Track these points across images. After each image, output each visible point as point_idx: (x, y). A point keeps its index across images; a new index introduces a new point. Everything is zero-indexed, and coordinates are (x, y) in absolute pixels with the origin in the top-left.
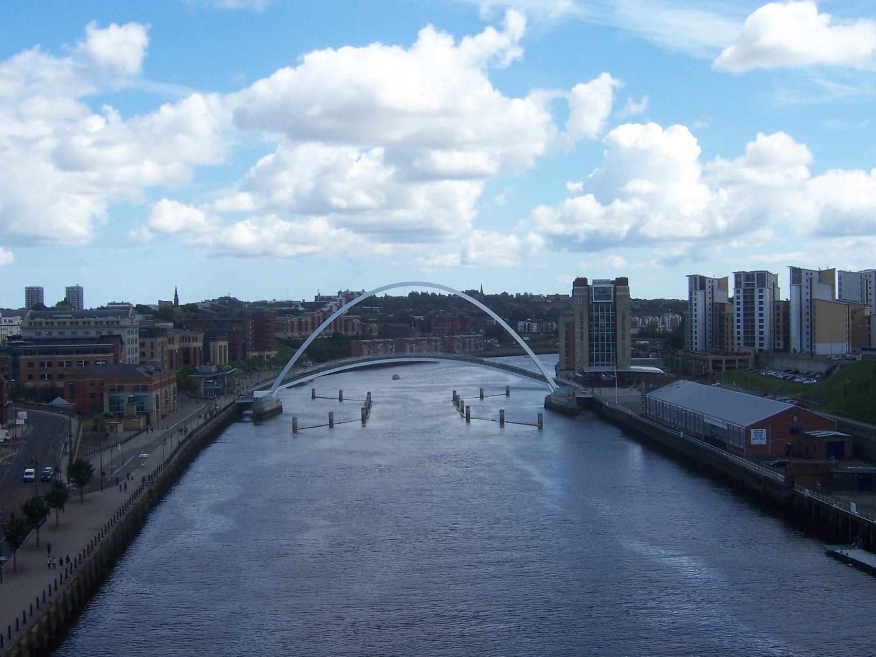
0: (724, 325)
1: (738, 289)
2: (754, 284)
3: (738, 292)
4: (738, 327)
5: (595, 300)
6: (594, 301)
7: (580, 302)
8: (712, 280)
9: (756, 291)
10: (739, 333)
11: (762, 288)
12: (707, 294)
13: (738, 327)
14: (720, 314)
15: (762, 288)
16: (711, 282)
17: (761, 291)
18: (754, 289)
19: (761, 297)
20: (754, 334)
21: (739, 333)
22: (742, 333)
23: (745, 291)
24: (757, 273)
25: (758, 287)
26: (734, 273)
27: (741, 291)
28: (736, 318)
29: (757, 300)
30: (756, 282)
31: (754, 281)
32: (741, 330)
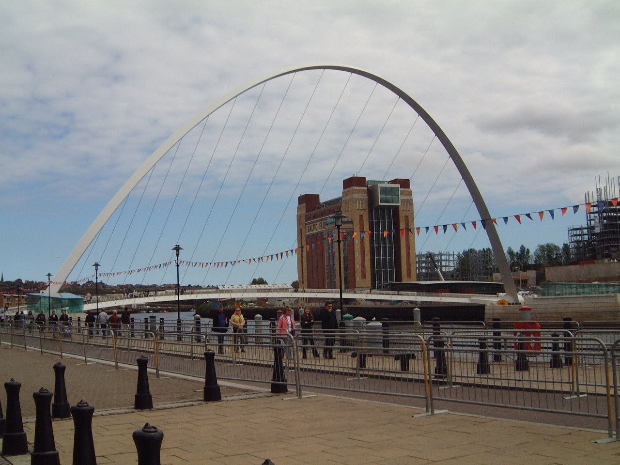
6: (380, 204)
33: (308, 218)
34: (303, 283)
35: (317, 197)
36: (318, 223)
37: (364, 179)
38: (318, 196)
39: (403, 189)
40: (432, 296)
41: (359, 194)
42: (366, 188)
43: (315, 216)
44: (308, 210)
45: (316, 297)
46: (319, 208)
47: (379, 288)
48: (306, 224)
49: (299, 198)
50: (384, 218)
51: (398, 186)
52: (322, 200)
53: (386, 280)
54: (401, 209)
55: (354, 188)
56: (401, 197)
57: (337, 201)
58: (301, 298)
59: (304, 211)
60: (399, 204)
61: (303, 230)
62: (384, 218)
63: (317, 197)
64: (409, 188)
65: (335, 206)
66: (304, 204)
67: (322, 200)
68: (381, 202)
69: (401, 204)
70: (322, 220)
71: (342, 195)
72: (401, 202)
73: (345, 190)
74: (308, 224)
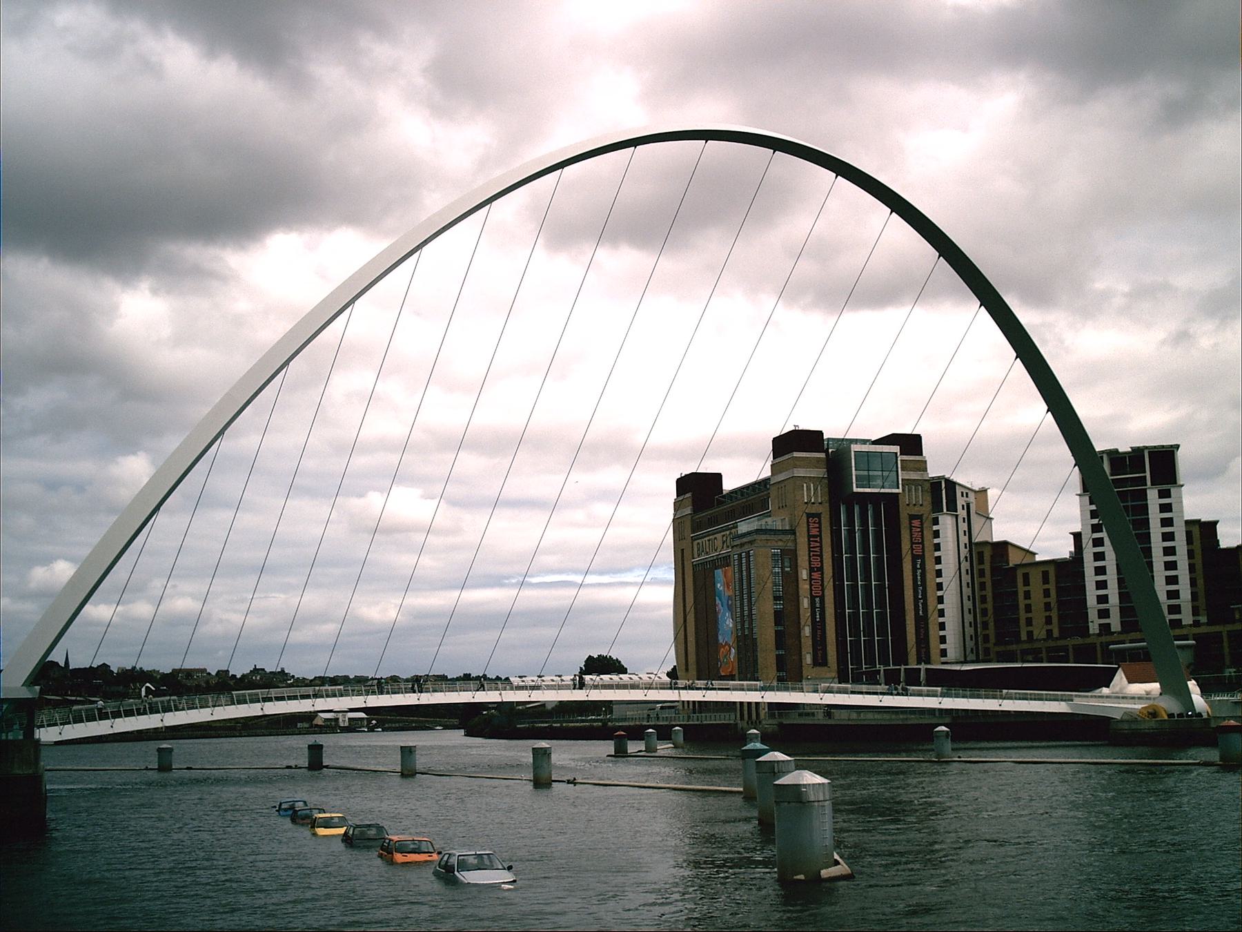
2: (1145, 477)
4: (1101, 585)
6: (855, 490)
7: (809, 495)
8: (967, 491)
9: (1152, 495)
10: (1103, 599)
12: (960, 520)
13: (1101, 585)
14: (994, 570)
15: (1165, 487)
16: (965, 495)
17: (1164, 494)
18: (1143, 495)
19: (1166, 508)
21: (1103, 599)
22: (1114, 599)
28: (1089, 565)
29: (1155, 516)
30: (1148, 474)
31: (1145, 472)
32: (1113, 592)
33: (696, 527)
34: (687, 670)
35: (718, 477)
36: (719, 536)
37: (820, 433)
39: (905, 458)
40: (979, 697)
41: (809, 468)
42: (823, 455)
43: (713, 521)
44: (698, 506)
45: (938, 706)
46: (720, 503)
47: (857, 680)
48: (693, 539)
51: (896, 449)
52: (728, 485)
54: (904, 500)
55: (796, 454)
57: (760, 487)
58: (688, 702)
59: (688, 511)
60: (900, 491)
61: (687, 554)
63: (718, 477)
64: (922, 455)
65: (754, 496)
66: (689, 495)
67: (728, 485)
68: (857, 487)
69: (903, 490)
70: (727, 528)
71: (770, 474)
72: (903, 485)
73: (778, 460)
74: (698, 538)
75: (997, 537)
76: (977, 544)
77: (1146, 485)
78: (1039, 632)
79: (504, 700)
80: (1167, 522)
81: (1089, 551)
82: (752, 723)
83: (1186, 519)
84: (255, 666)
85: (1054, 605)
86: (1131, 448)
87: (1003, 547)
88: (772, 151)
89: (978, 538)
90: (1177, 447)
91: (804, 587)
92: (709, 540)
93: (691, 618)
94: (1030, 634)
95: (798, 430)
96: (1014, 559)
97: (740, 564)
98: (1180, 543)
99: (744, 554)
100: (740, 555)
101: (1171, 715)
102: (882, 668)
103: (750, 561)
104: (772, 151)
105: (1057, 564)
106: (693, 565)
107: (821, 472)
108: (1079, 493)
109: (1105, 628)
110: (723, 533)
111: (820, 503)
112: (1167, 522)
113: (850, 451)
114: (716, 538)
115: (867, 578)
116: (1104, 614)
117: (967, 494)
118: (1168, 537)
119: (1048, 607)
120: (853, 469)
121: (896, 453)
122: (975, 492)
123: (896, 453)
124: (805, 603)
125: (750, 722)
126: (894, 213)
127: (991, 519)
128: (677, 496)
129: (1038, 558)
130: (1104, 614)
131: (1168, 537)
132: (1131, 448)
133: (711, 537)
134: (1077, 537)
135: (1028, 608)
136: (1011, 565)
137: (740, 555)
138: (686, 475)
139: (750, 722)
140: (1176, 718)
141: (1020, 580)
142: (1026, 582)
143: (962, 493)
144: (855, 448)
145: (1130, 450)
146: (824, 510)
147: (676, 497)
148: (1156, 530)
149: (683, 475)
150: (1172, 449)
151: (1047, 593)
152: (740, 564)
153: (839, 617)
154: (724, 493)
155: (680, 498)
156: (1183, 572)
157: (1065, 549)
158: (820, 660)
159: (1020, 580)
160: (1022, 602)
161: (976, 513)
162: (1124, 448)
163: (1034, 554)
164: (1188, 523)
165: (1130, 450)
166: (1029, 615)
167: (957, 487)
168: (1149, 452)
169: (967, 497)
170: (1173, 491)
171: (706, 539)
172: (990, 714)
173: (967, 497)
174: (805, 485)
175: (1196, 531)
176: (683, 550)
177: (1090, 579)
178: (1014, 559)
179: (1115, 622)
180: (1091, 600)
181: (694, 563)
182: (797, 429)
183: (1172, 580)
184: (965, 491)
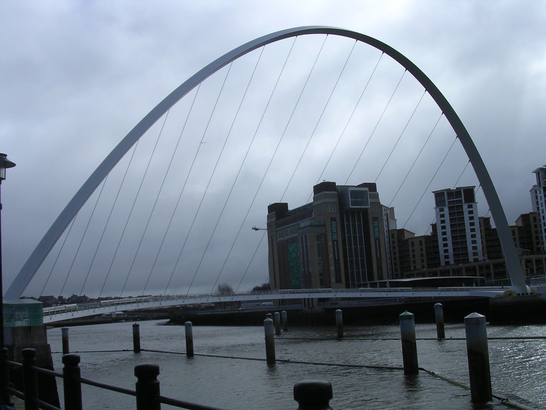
0: (408, 250)
1: (440, 208)
3: (442, 210)
5: (352, 205)
6: (351, 207)
7: (331, 211)
9: (465, 206)
10: (446, 251)
11: (471, 204)
14: (399, 241)
15: (471, 204)
17: (470, 206)
18: (462, 206)
19: (471, 212)
20: (467, 251)
21: (446, 251)
22: (451, 251)
23: (449, 208)
24: (464, 190)
25: (466, 202)
26: (433, 192)
27: (446, 209)
28: (440, 237)
29: (466, 216)
31: (462, 198)
32: (450, 248)
35: (286, 205)
37: (335, 183)
38: (287, 204)
39: (370, 193)
42: (336, 193)
46: (288, 215)
47: (354, 286)
49: (269, 207)
50: (354, 221)
51: (367, 189)
52: (291, 208)
53: (358, 280)
55: (326, 192)
56: (369, 200)
58: (277, 300)
59: (274, 219)
60: (369, 207)
62: (354, 221)
63: (286, 205)
64: (376, 192)
66: (274, 212)
67: (291, 208)
68: (352, 205)
71: (313, 201)
75: (399, 227)
76: (391, 230)
77: (462, 203)
78: (419, 266)
79: (221, 301)
80: (471, 218)
81: (439, 231)
82: (310, 308)
83: (479, 216)
84: (73, 294)
85: (425, 254)
86: (456, 188)
87: (402, 231)
88: (356, 40)
89: (391, 228)
90: (475, 187)
91: (331, 249)
92: (284, 232)
93: (277, 266)
94: (415, 267)
95: (325, 182)
96: (407, 236)
97: (302, 241)
98: (477, 226)
99: (304, 236)
100: (302, 237)
101: (519, 294)
102: (378, 281)
103: (307, 239)
104: (356, 40)
105: (426, 238)
106: (277, 243)
107: (336, 200)
108: (435, 207)
109: (447, 263)
110: (291, 228)
111: (336, 213)
112: (471, 218)
113: (348, 190)
114: (287, 230)
115: (356, 244)
116: (447, 257)
117: (386, 209)
118: (472, 224)
119: (422, 255)
120: (350, 198)
121: (367, 191)
122: (390, 209)
123: (367, 191)
124: (331, 256)
125: (309, 308)
126: (407, 71)
127: (396, 220)
128: (269, 213)
129: (416, 236)
130: (447, 257)
131: (472, 224)
132: (456, 188)
133: (285, 230)
134: (434, 226)
135: (414, 256)
136: (406, 238)
137: (302, 237)
138: (272, 204)
139: (309, 308)
140: (525, 295)
141: (410, 245)
142: (413, 245)
143: (385, 209)
144: (350, 189)
145: (455, 189)
146: (337, 216)
147: (268, 214)
148: (467, 222)
149: (271, 204)
150: (472, 188)
151: (421, 250)
152: (302, 241)
153: (345, 262)
154: (289, 211)
155: (270, 214)
156: (478, 239)
157: (428, 232)
158: (338, 281)
159: (410, 245)
160: (411, 254)
161: (390, 218)
162: (453, 188)
163: (414, 234)
164: (480, 218)
165: (455, 189)
166: (414, 259)
167: (383, 207)
168: (463, 189)
169: (386, 211)
170: (474, 205)
171: (283, 231)
172: (438, 298)
173: (386, 211)
174: (329, 205)
175: (482, 221)
176: (272, 236)
177: (441, 243)
178: (407, 236)
179: (451, 261)
180: (442, 252)
181: (278, 242)
182: (325, 181)
183: (474, 242)
184: (385, 208)
